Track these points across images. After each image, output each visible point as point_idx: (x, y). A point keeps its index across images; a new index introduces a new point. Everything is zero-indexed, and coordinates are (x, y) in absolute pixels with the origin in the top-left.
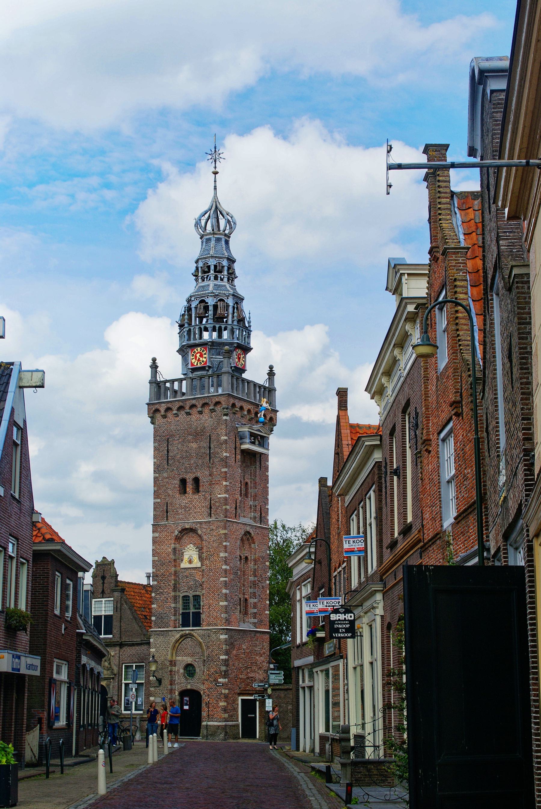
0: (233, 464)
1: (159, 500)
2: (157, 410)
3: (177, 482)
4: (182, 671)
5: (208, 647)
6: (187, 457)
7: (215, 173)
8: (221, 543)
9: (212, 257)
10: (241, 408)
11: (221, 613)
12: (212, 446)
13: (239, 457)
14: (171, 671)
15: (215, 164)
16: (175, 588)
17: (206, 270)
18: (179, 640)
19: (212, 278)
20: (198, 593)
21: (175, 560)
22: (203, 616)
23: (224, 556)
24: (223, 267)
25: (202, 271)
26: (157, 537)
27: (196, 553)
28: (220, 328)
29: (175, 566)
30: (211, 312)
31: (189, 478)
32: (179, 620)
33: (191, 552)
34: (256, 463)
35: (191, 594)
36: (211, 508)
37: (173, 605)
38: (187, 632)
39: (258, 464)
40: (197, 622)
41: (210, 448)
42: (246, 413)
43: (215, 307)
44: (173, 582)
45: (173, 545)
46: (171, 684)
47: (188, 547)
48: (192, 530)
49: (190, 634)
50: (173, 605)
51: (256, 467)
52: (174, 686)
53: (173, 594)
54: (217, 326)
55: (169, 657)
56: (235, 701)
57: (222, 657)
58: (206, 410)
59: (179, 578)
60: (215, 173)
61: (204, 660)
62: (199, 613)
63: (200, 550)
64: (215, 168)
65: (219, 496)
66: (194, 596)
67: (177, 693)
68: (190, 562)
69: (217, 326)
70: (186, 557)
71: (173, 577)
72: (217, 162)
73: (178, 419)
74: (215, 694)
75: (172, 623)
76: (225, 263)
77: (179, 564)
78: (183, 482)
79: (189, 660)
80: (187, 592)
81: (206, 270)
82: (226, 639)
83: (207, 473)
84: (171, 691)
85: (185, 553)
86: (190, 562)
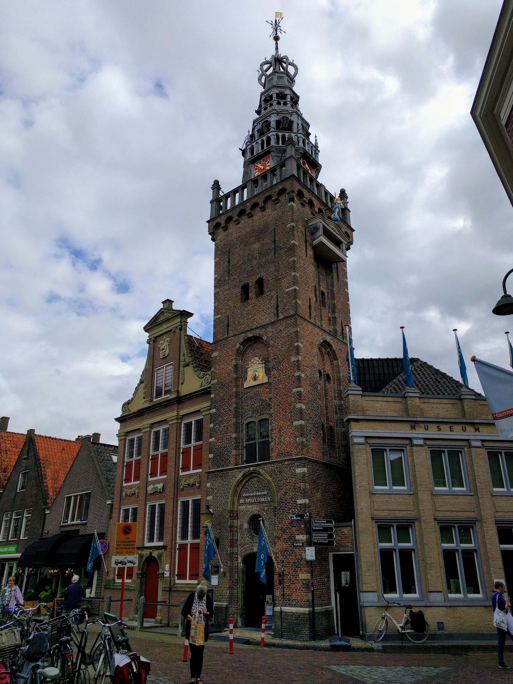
0: (304, 256)
1: (219, 316)
2: (218, 226)
3: (238, 290)
4: (246, 526)
5: (279, 488)
6: (249, 260)
8: (291, 344)
9: (274, 86)
11: (296, 437)
12: (277, 239)
14: (231, 527)
16: (237, 414)
18: (241, 481)
19: (275, 103)
20: (265, 416)
21: (236, 379)
22: (272, 444)
23: (295, 360)
27: (260, 366)
28: (283, 137)
29: (237, 386)
31: (252, 282)
32: (242, 455)
33: (255, 366)
34: (332, 272)
36: (278, 306)
37: (234, 435)
38: (252, 469)
39: (335, 274)
41: (275, 241)
42: (317, 210)
44: (234, 406)
45: (234, 362)
46: (232, 546)
47: (252, 360)
48: (257, 339)
49: (254, 472)
50: (234, 435)
51: (332, 277)
52: (235, 550)
53: (234, 420)
54: (280, 134)
55: (229, 507)
57: (299, 502)
58: (269, 205)
59: (242, 401)
61: (275, 508)
62: (268, 443)
63: (266, 361)
64: (276, 34)
65: (287, 290)
66: (260, 421)
67: (240, 559)
68: (255, 378)
69: (280, 134)
70: (250, 374)
71: (234, 400)
73: (239, 225)
74: (291, 559)
75: (232, 460)
77: (243, 384)
78: (245, 288)
79: (255, 509)
80: (252, 416)
82: (304, 472)
83: (272, 269)
84: (232, 556)
85: (248, 370)
86: (255, 378)
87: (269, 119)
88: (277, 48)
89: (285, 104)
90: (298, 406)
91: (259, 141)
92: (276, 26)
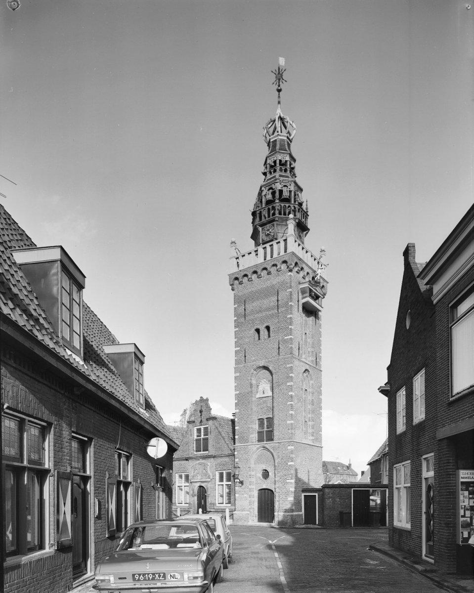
3: (253, 331)
7: (279, 91)
10: (302, 269)
13: (301, 309)
15: (279, 83)
17: (273, 164)
24: (286, 161)
25: (271, 168)
26: (238, 377)
35: (265, 417)
40: (270, 438)
56: (301, 496)
60: (279, 91)
64: (279, 86)
65: (286, 338)
70: (261, 388)
72: (281, 82)
78: (258, 331)
87: (273, 186)
88: (279, 97)
89: (286, 171)
90: (291, 412)
91: (267, 209)
92: (279, 75)
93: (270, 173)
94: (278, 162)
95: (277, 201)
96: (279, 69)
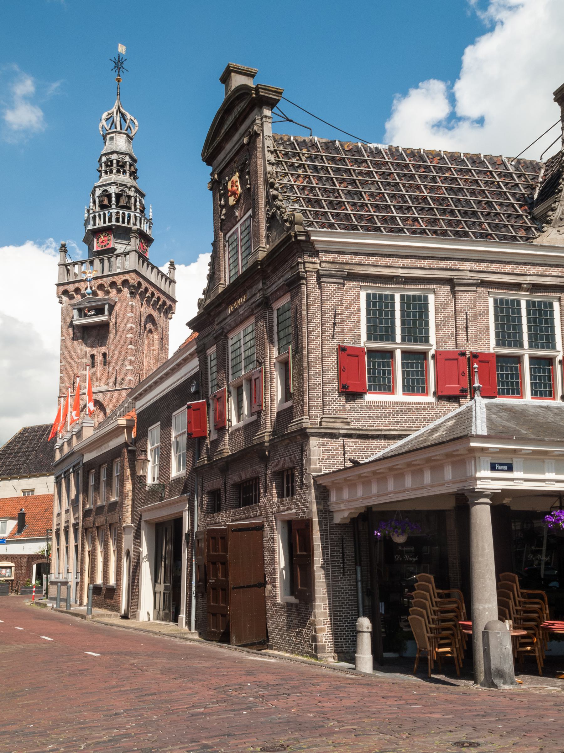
19: (115, 171)
24: (126, 162)
30: (114, 199)
43: (118, 196)
69: (121, 212)
76: (127, 159)
81: (109, 164)
89: (124, 172)
93: (106, 172)
94: (115, 162)
95: (114, 206)
96: (119, 57)
